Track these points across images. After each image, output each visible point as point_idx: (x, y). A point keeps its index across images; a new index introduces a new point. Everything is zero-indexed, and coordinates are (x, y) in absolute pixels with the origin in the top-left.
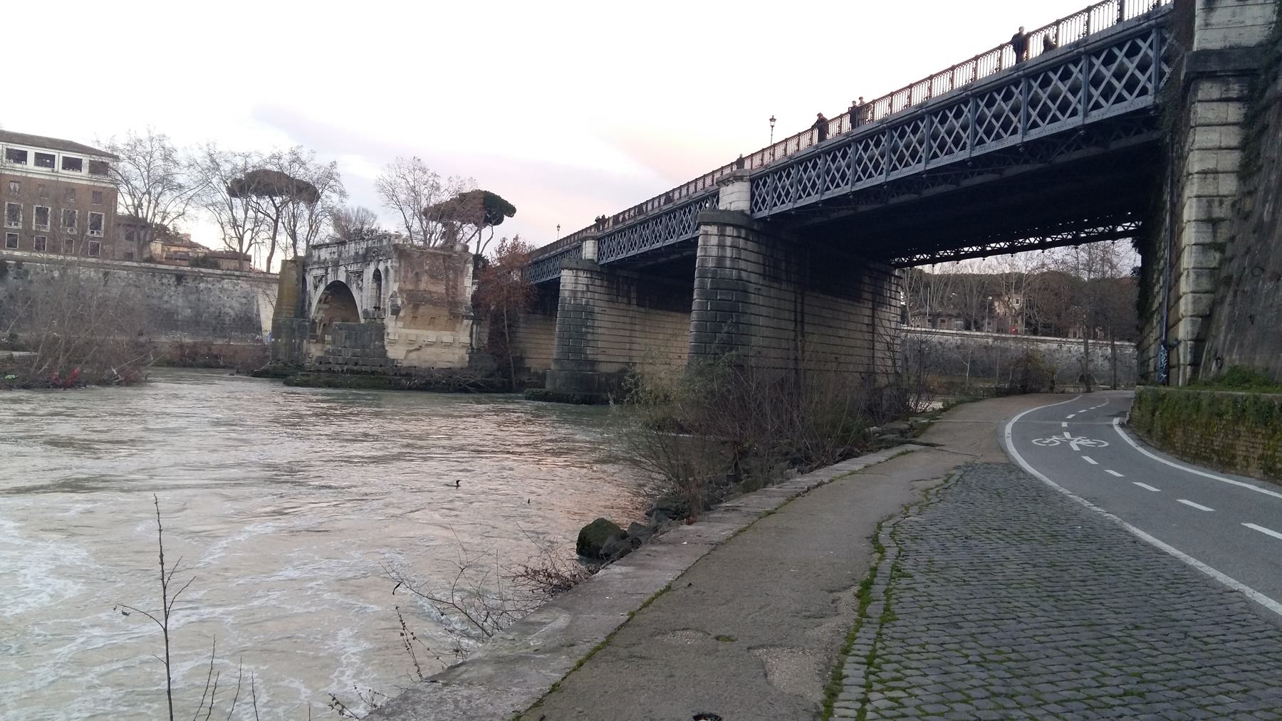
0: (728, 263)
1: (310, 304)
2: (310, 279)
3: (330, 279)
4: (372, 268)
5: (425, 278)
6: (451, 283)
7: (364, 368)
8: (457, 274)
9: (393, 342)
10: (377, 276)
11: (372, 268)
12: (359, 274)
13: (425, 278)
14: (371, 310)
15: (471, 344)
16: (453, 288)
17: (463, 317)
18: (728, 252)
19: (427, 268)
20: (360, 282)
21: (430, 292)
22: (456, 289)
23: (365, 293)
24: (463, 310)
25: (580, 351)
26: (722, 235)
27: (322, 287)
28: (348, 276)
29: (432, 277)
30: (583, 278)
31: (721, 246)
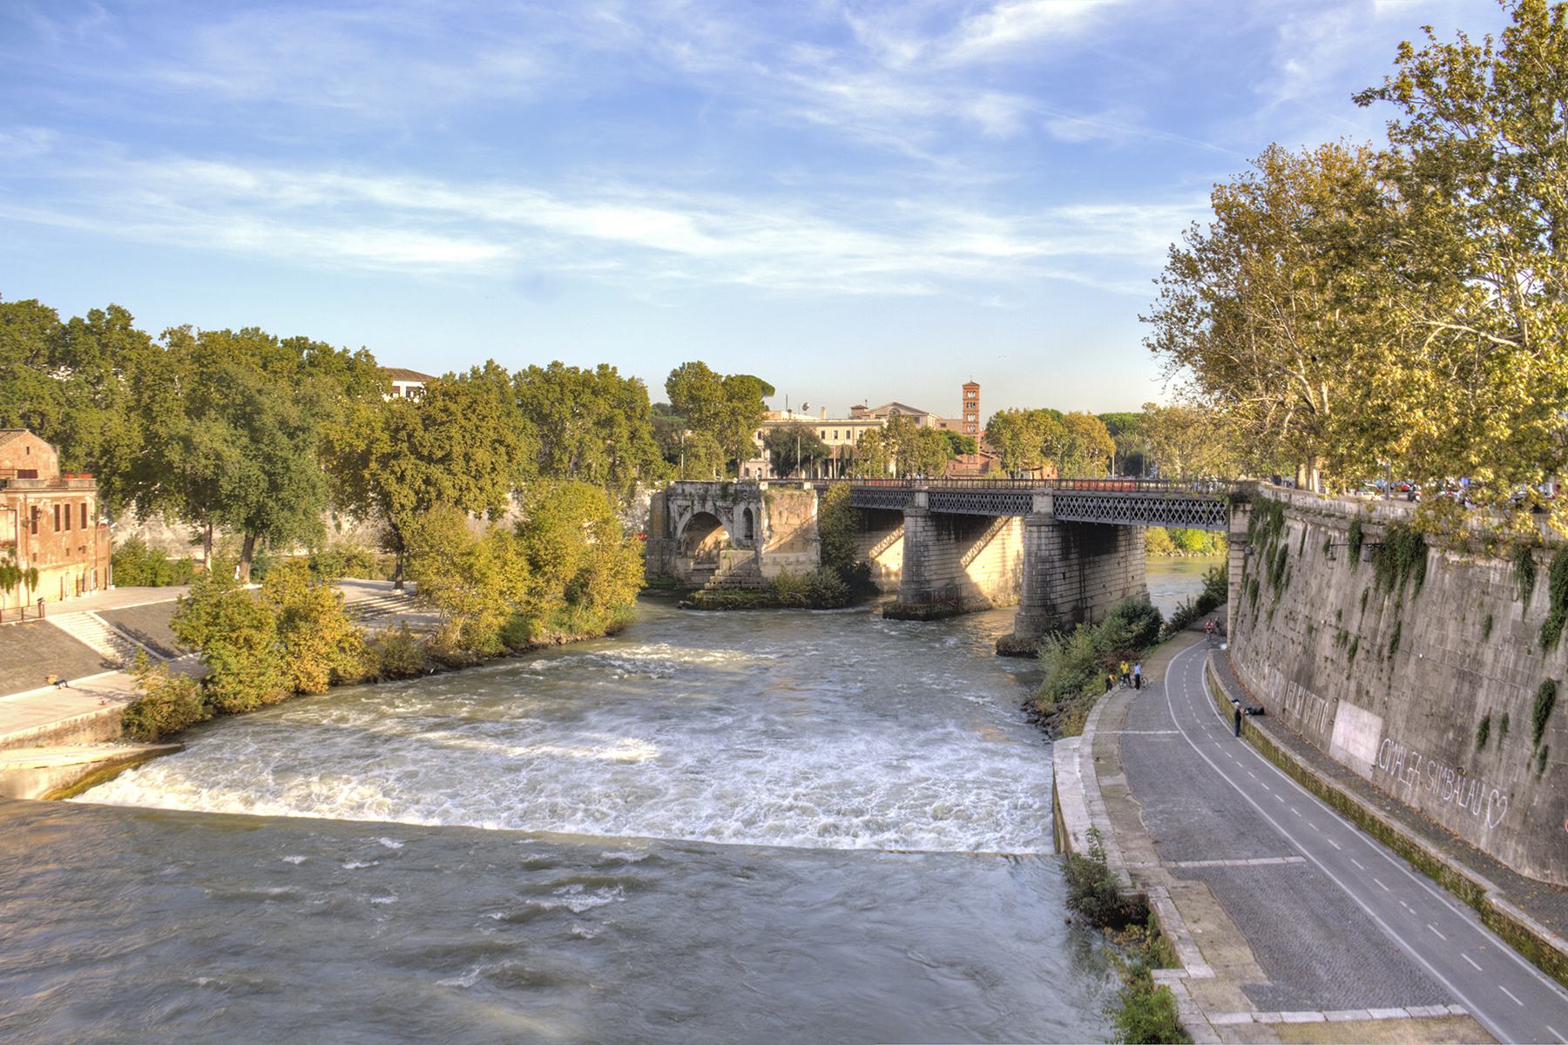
0: (1043, 547)
1: (675, 528)
2: (673, 507)
3: (697, 509)
4: (742, 507)
9: (765, 565)
10: (748, 513)
11: (742, 507)
12: (730, 510)
13: (785, 514)
14: (742, 538)
18: (1043, 541)
23: (736, 525)
25: (920, 575)
26: (1039, 532)
27: (687, 516)
28: (716, 510)
30: (921, 522)
31: (1039, 538)
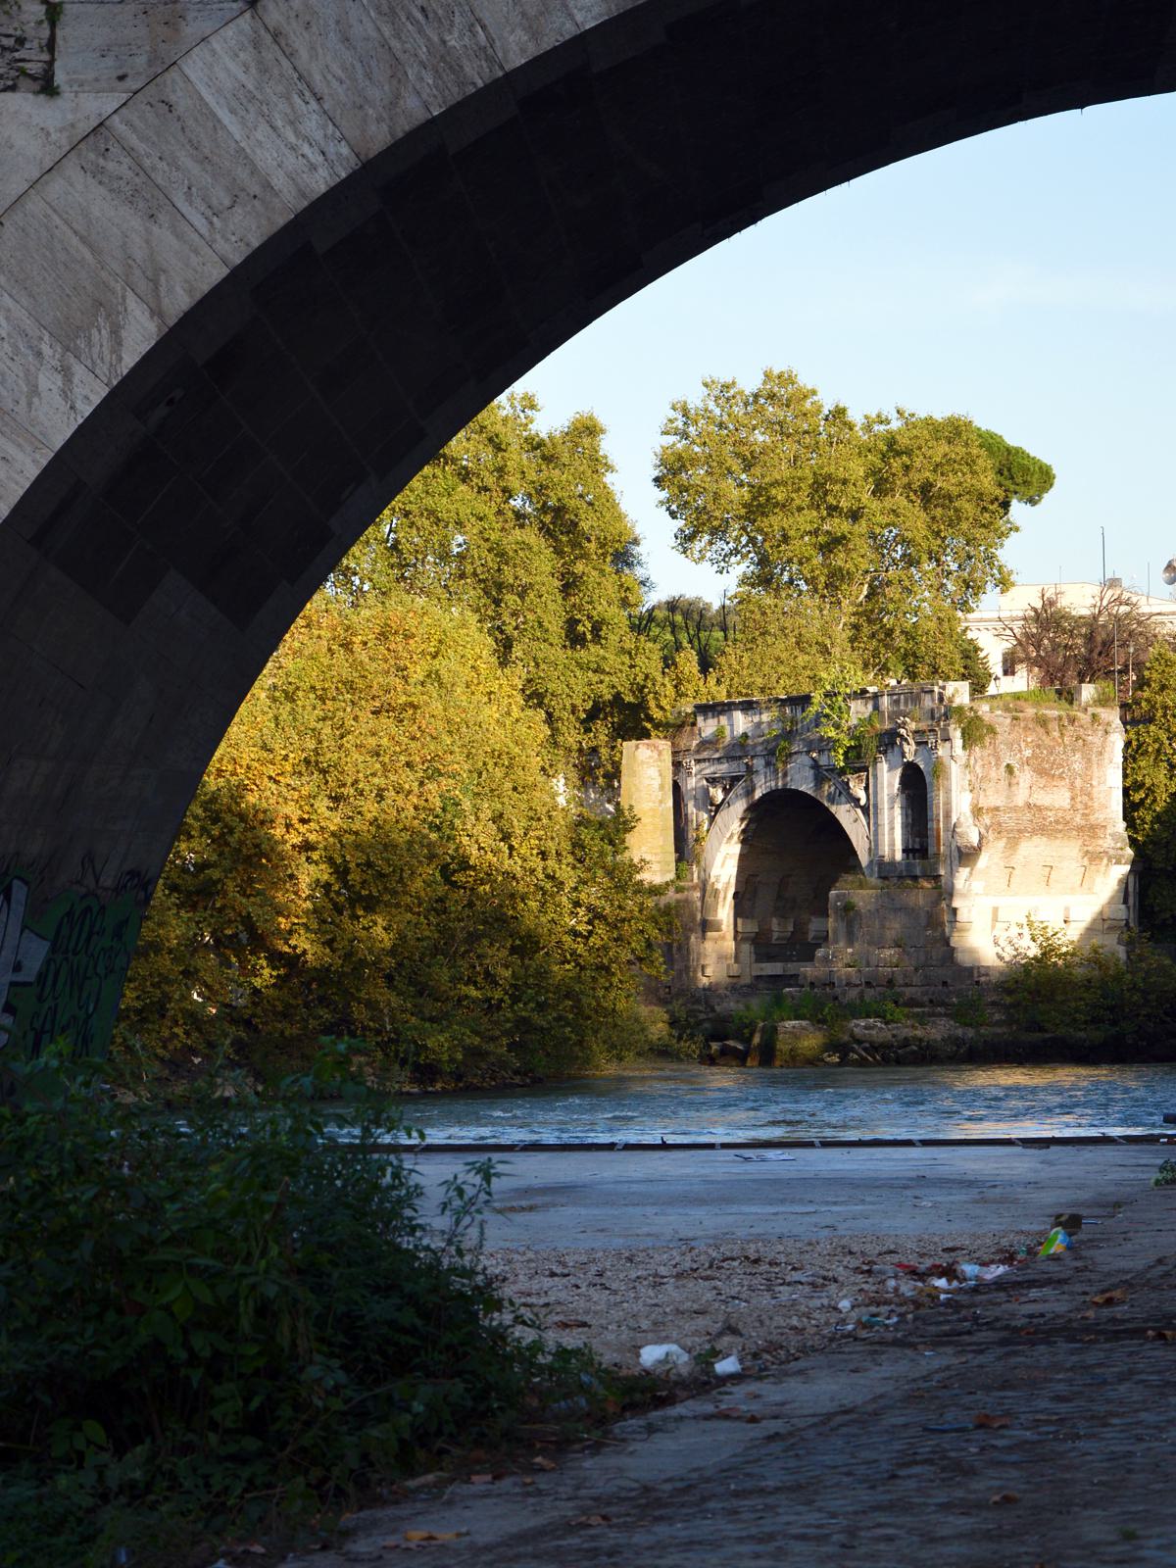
5: (1025, 777)
6: (1078, 783)
7: (908, 992)
8: (1089, 760)
13: (1025, 777)
15: (1127, 924)
16: (1083, 795)
17: (1109, 860)
19: (1028, 753)
20: (861, 795)
21: (1039, 809)
22: (1089, 795)
24: (1107, 843)
29: (1041, 772)
